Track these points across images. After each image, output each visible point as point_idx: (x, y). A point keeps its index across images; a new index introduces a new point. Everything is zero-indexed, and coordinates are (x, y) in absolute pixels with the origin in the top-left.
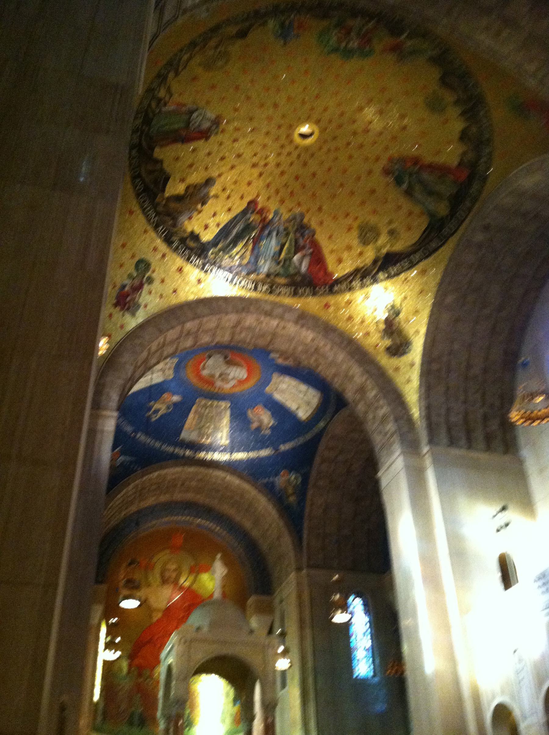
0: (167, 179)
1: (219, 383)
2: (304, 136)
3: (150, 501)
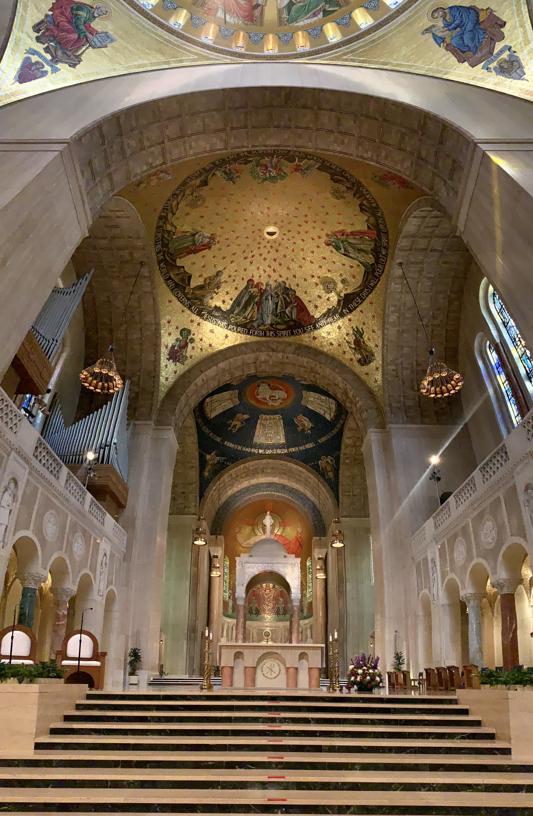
0: (190, 277)
1: (271, 403)
2: (271, 234)
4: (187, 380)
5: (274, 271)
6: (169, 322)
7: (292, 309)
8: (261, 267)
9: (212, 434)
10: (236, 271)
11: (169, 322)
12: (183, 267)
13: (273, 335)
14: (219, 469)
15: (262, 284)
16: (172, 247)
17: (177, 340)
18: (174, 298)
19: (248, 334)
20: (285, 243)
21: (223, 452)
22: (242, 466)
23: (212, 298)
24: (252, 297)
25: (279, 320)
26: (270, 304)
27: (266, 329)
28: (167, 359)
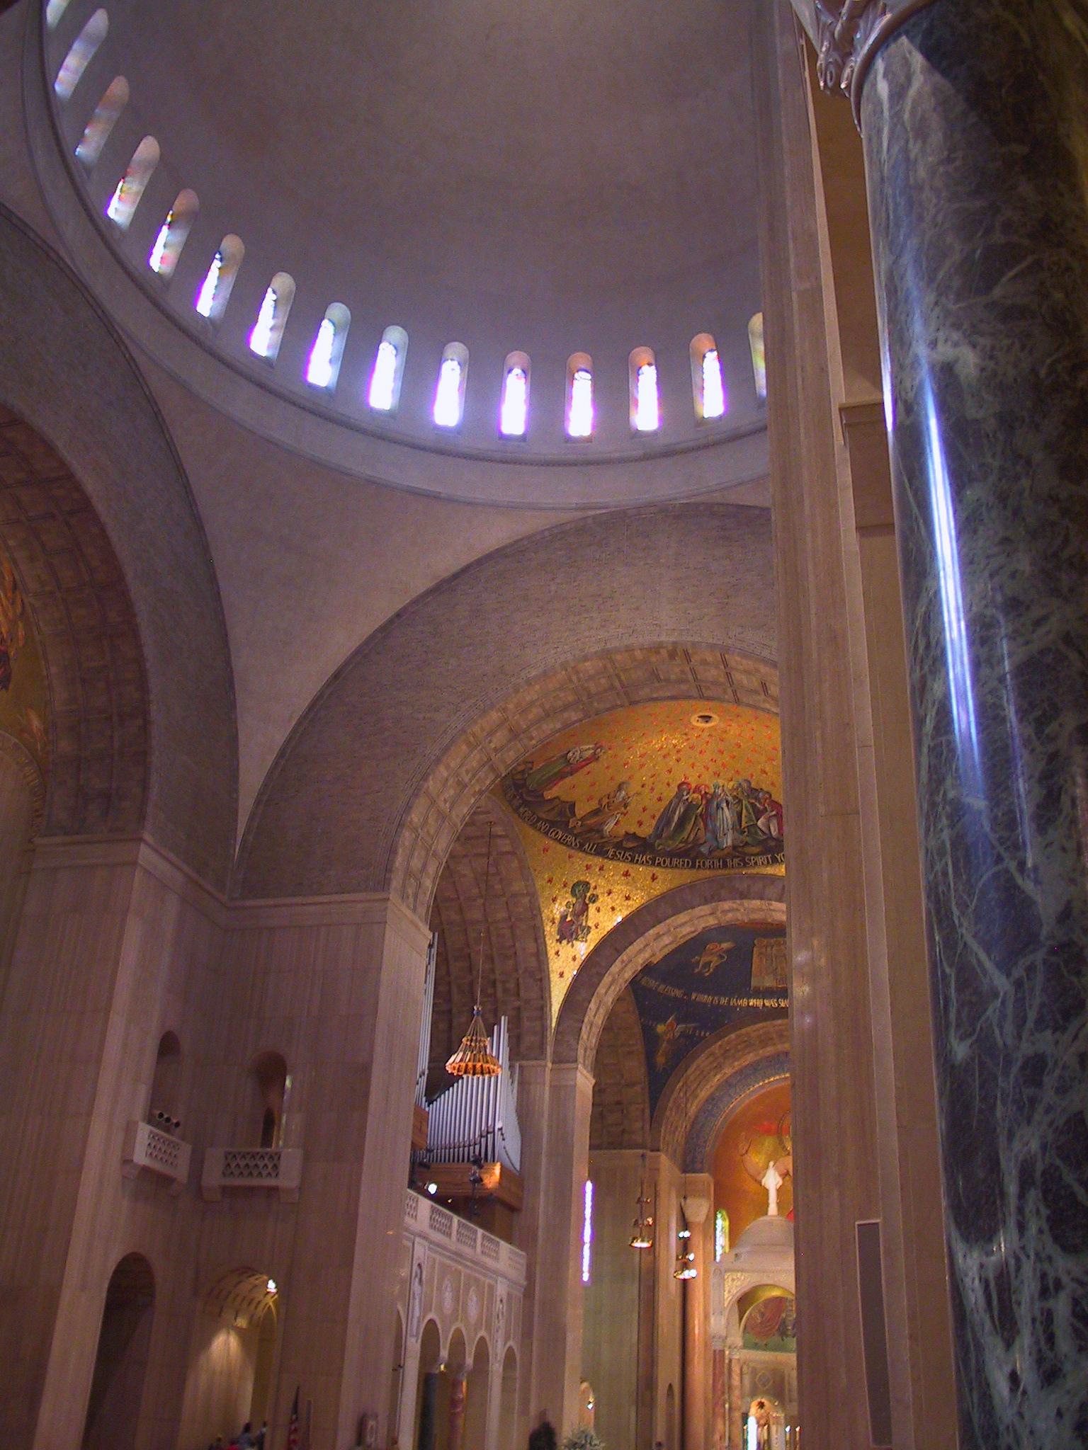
0: (573, 806)
4: (594, 971)
11: (550, 881)
14: (685, 1050)
17: (568, 905)
19: (693, 866)
21: (686, 1011)
26: (727, 815)
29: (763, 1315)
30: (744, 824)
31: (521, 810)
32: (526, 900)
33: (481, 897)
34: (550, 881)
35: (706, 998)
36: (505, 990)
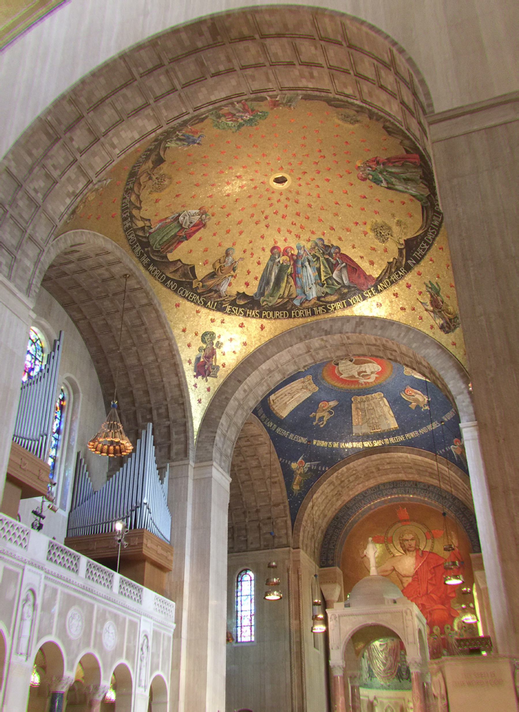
0: (193, 269)
3: (360, 489)
5: (302, 227)
6: (184, 330)
7: (340, 271)
8: (282, 229)
9: (292, 435)
10: (251, 242)
12: (179, 260)
13: (323, 311)
15: (292, 248)
16: (156, 242)
17: (200, 349)
18: (181, 301)
19: (290, 317)
20: (304, 189)
21: (312, 454)
22: (344, 469)
23: (230, 285)
24: (282, 269)
25: (328, 290)
27: (313, 305)
28: (195, 376)
29: (384, 664)
30: (323, 278)
31: (151, 268)
32: (166, 343)
33: (134, 345)
34: (184, 330)
35: (323, 444)
36: (159, 415)
